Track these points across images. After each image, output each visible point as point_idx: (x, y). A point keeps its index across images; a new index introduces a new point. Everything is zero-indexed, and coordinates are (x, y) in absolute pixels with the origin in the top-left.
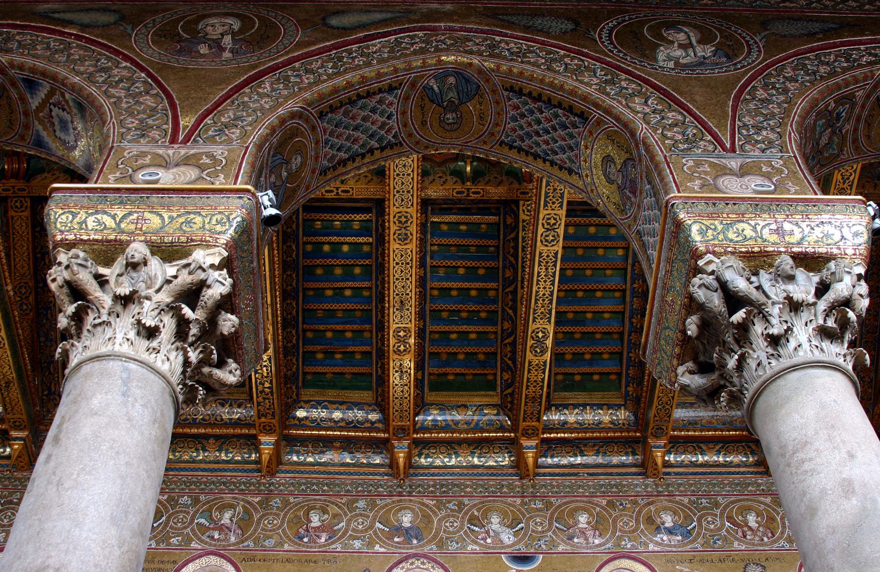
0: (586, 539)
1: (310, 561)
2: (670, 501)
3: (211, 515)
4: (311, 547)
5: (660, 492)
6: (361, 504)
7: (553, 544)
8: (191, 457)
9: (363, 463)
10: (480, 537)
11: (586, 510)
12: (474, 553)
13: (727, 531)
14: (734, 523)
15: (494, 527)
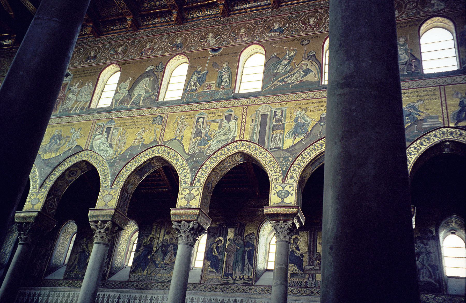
0: (242, 39)
1: (143, 61)
2: (280, 18)
3: (115, 50)
4: (145, 56)
5: (277, 14)
6: (165, 37)
7: (229, 42)
8: (112, 29)
9: (169, 21)
10: (203, 44)
11: (244, 27)
12: (199, 50)
13: (300, 28)
14: (304, 24)
15: (208, 39)
